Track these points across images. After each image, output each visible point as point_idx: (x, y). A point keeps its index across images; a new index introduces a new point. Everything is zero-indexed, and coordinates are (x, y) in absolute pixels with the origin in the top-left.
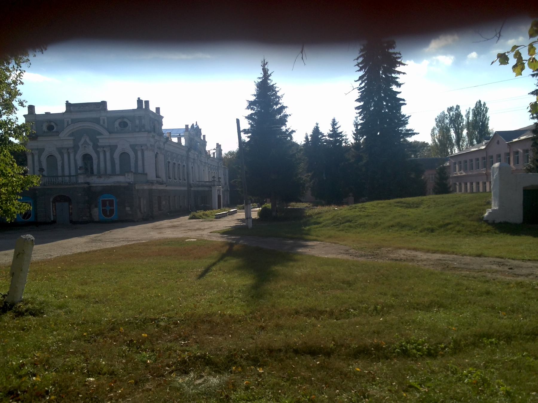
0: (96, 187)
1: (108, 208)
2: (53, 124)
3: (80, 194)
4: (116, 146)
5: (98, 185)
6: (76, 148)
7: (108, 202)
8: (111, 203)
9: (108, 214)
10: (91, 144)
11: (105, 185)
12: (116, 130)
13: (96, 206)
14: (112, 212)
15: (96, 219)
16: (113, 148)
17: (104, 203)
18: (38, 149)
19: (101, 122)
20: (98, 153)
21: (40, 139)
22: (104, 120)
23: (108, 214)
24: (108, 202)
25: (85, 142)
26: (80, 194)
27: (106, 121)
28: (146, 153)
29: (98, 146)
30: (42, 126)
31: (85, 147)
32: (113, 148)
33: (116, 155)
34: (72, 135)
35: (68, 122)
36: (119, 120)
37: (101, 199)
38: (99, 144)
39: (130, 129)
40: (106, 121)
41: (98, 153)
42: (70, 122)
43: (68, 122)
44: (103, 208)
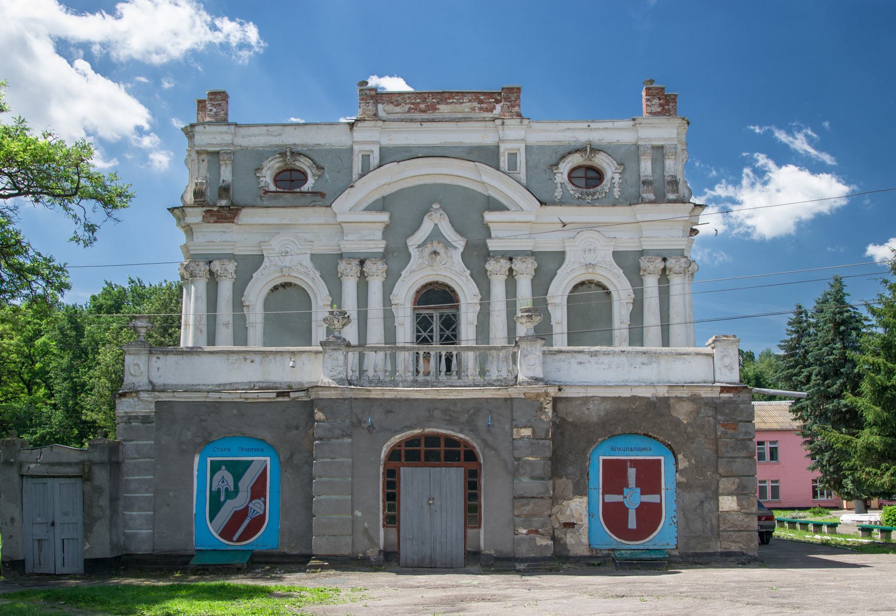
0: (586, 400)
1: (633, 498)
2: (303, 164)
3: (526, 432)
4: (560, 257)
5: (591, 392)
6: (395, 256)
7: (632, 473)
8: (649, 477)
9: (632, 524)
10: (460, 243)
11: (626, 393)
12: (558, 194)
13: (581, 490)
14: (650, 516)
15: (577, 543)
16: (547, 264)
17: (615, 475)
18: (232, 257)
19: (504, 162)
20: (482, 280)
21: (247, 216)
22: (513, 156)
23: (632, 524)
24: (632, 473)
25: (436, 235)
26: (526, 432)
27: (521, 159)
28: (677, 284)
29: (488, 255)
30: (259, 169)
31: (435, 253)
32: (547, 264)
33: (559, 292)
34: (381, 205)
35: (366, 158)
36: (576, 160)
37: (599, 457)
38: (493, 245)
39: (616, 193)
40: (521, 159)
41: (482, 280)
42: (375, 160)
43: (366, 158)
44: (612, 498)
